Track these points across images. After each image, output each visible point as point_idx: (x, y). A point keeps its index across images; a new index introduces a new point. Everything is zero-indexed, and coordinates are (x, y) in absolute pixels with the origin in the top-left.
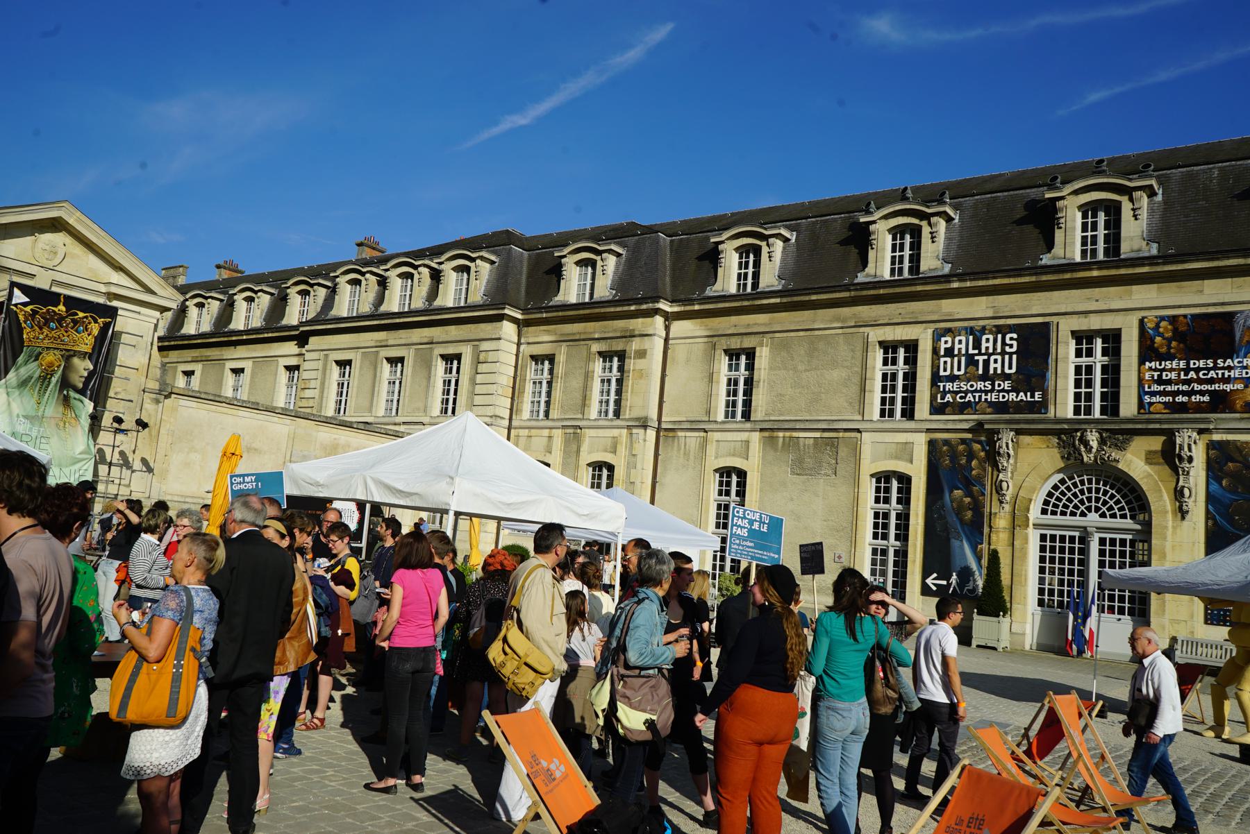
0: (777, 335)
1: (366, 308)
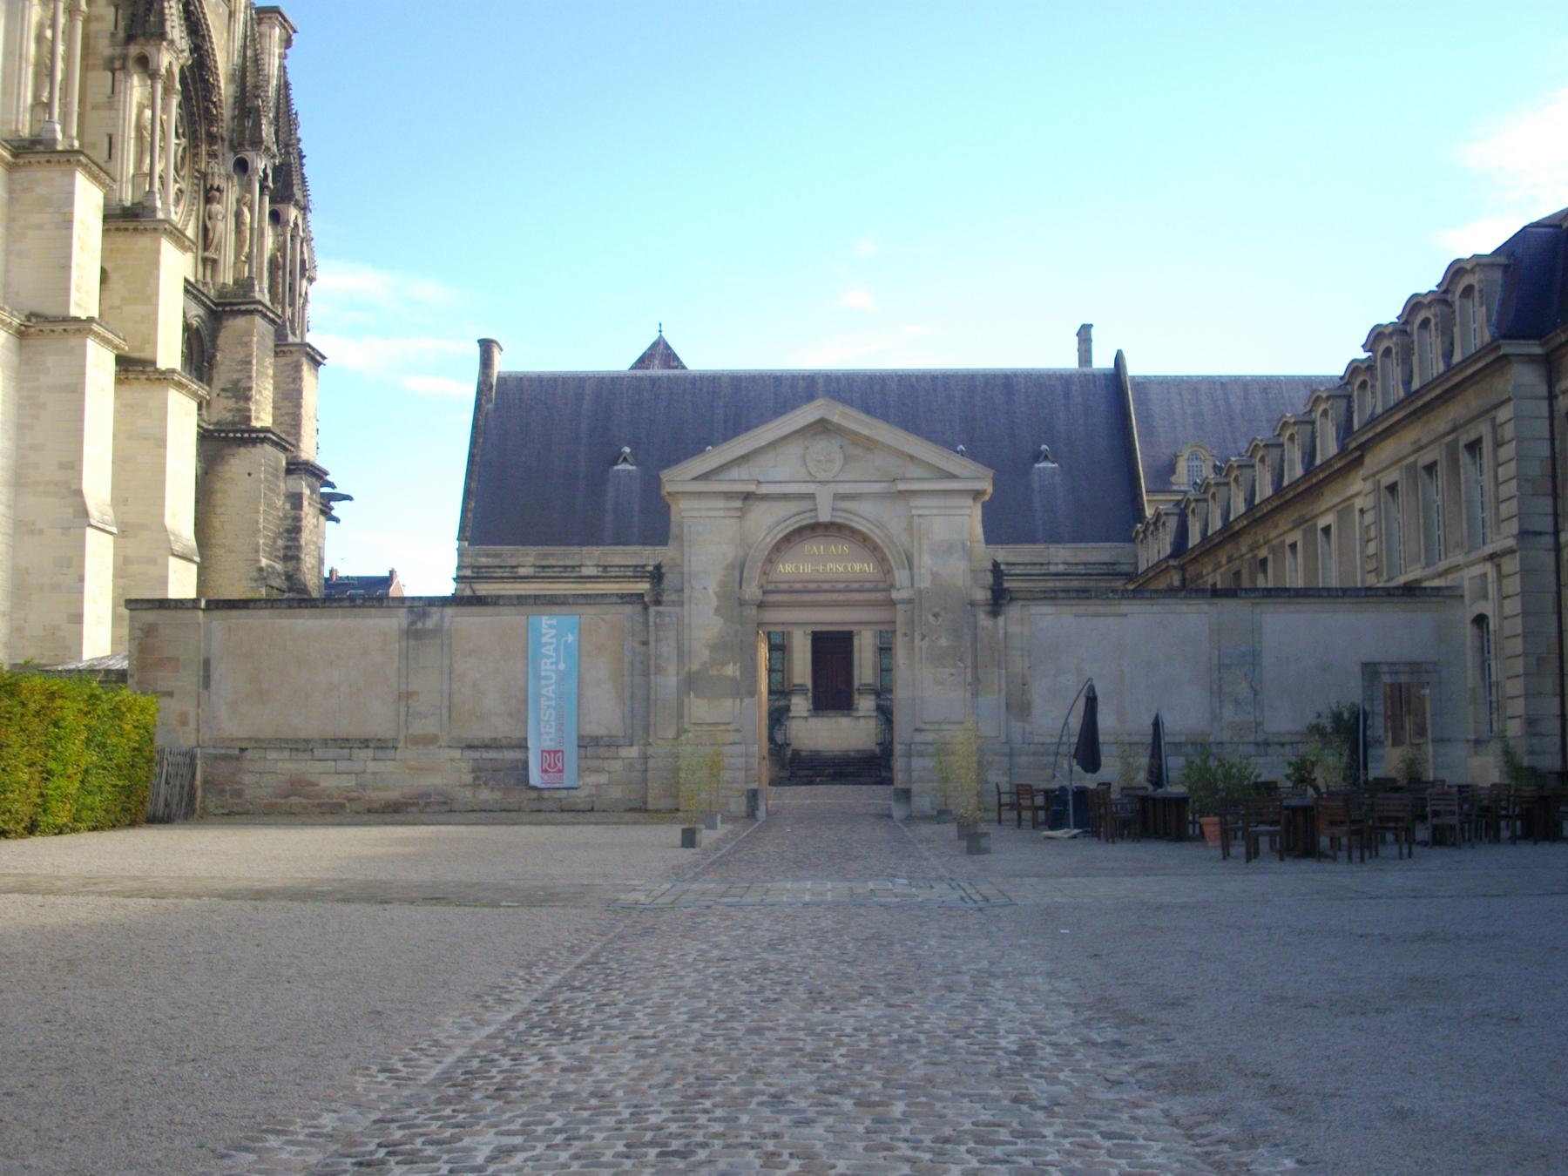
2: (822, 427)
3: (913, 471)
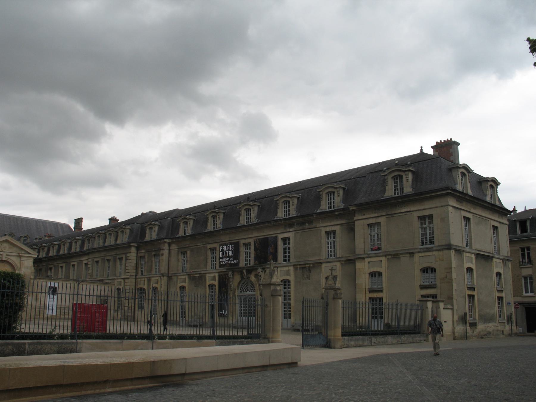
0: (191, 247)
1: (101, 244)
2: (6, 241)
3: (23, 252)
